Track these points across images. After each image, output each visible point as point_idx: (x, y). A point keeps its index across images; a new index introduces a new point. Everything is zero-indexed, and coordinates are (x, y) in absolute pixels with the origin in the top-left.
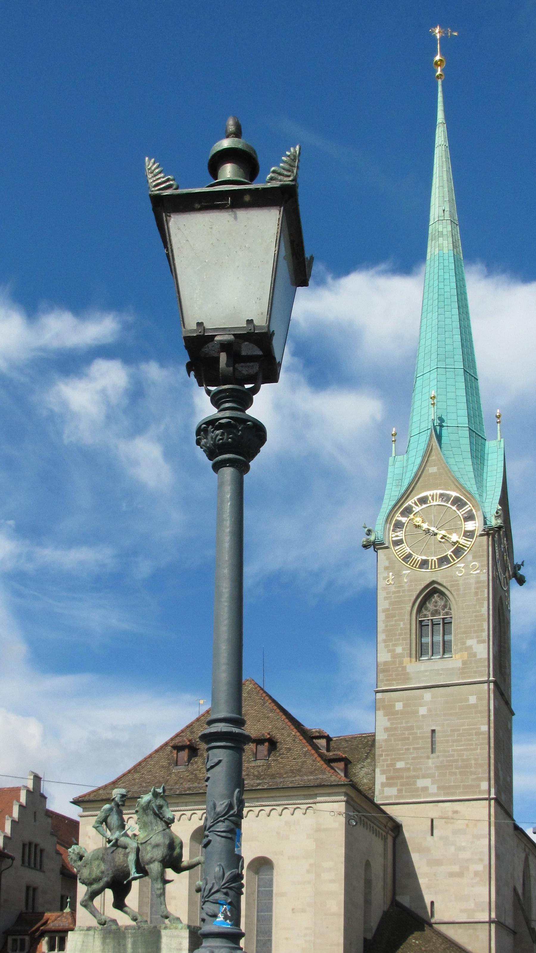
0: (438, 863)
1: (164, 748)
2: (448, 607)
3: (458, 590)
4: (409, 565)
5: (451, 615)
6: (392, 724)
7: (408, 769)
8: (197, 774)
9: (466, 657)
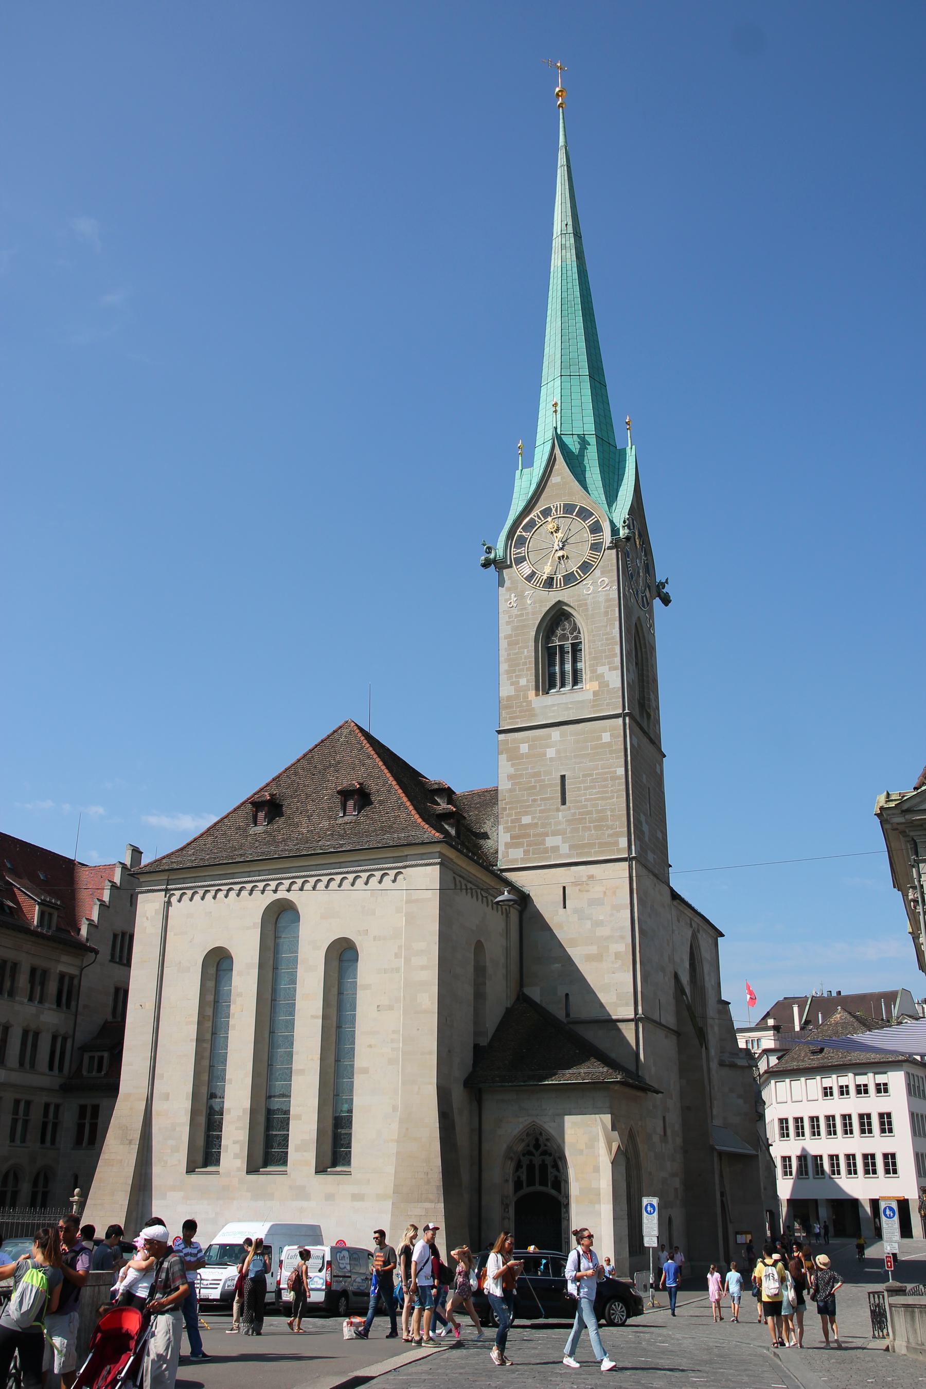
3: (587, 610)
4: (533, 584)
5: (580, 639)
6: (516, 770)
7: (535, 825)
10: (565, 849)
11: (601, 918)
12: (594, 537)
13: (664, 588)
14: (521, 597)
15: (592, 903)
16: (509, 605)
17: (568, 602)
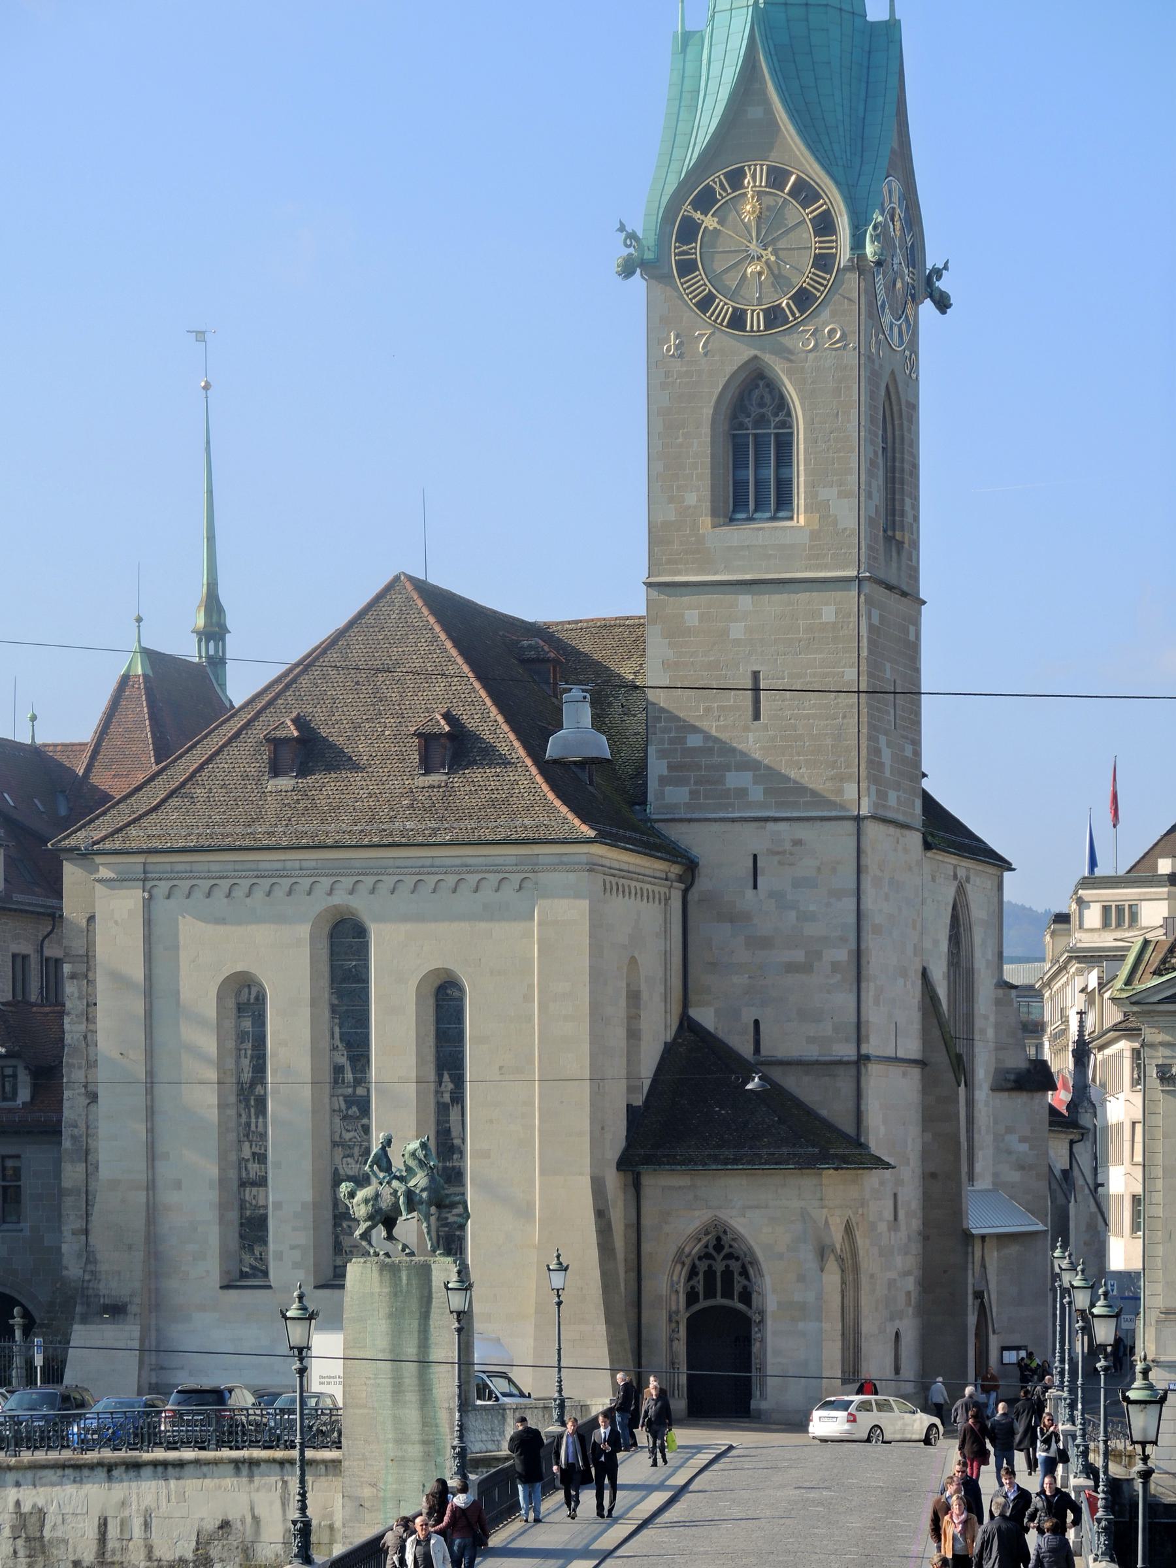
0: (765, 943)
2: (784, 413)
4: (710, 318)
10: (757, 793)
11: (812, 908)
12: (820, 242)
13: (939, 278)
15: (797, 884)
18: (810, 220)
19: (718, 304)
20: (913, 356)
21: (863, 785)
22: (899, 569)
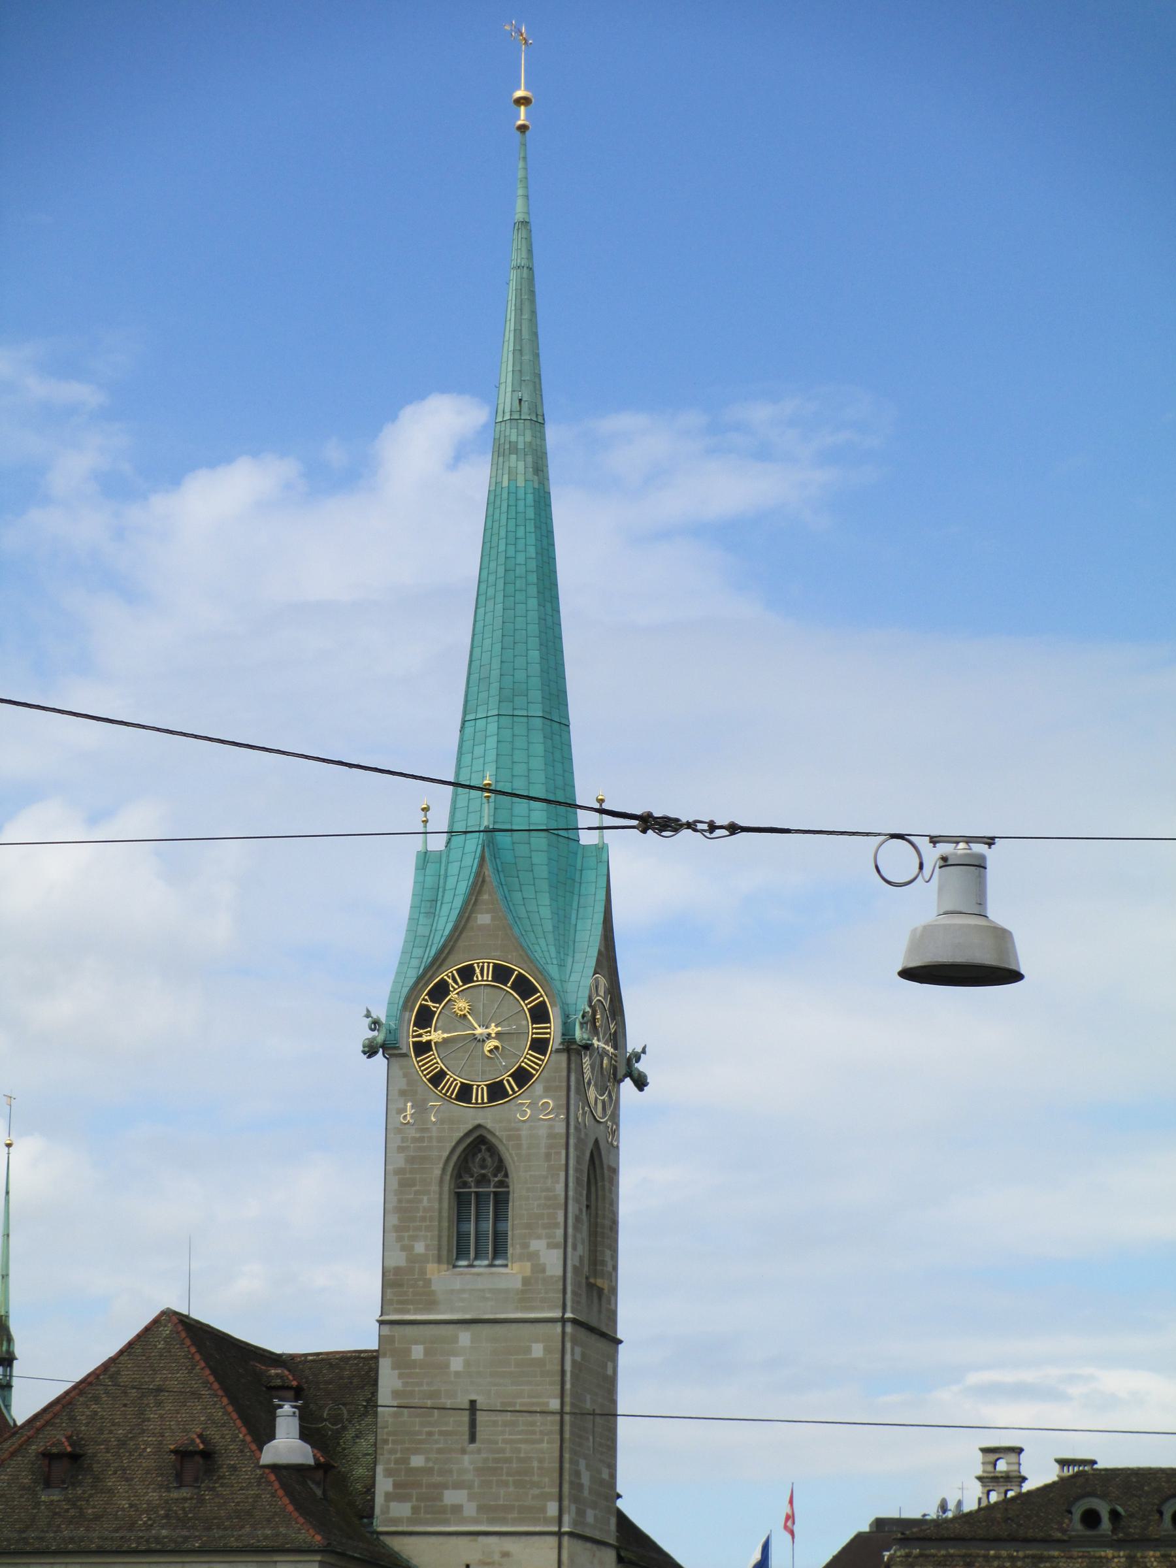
1: (24, 1447)
2: (503, 1173)
3: (519, 1147)
4: (441, 1092)
6: (405, 1384)
7: (429, 1471)
8: (84, 1507)
9: (528, 1273)
10: (470, 1509)
13: (637, 1061)
14: (421, 1109)
16: (402, 1120)
17: (492, 1130)
18: (528, 1009)
19: (449, 1080)
20: (614, 1127)
21: (566, 1503)
22: (600, 1311)
